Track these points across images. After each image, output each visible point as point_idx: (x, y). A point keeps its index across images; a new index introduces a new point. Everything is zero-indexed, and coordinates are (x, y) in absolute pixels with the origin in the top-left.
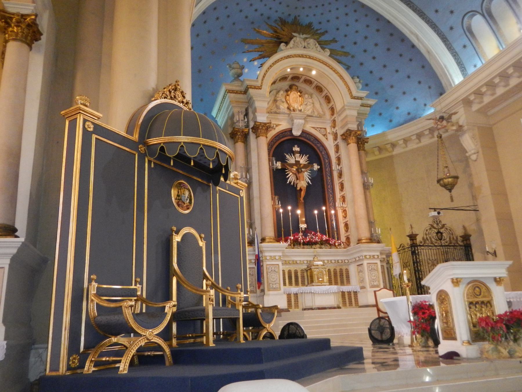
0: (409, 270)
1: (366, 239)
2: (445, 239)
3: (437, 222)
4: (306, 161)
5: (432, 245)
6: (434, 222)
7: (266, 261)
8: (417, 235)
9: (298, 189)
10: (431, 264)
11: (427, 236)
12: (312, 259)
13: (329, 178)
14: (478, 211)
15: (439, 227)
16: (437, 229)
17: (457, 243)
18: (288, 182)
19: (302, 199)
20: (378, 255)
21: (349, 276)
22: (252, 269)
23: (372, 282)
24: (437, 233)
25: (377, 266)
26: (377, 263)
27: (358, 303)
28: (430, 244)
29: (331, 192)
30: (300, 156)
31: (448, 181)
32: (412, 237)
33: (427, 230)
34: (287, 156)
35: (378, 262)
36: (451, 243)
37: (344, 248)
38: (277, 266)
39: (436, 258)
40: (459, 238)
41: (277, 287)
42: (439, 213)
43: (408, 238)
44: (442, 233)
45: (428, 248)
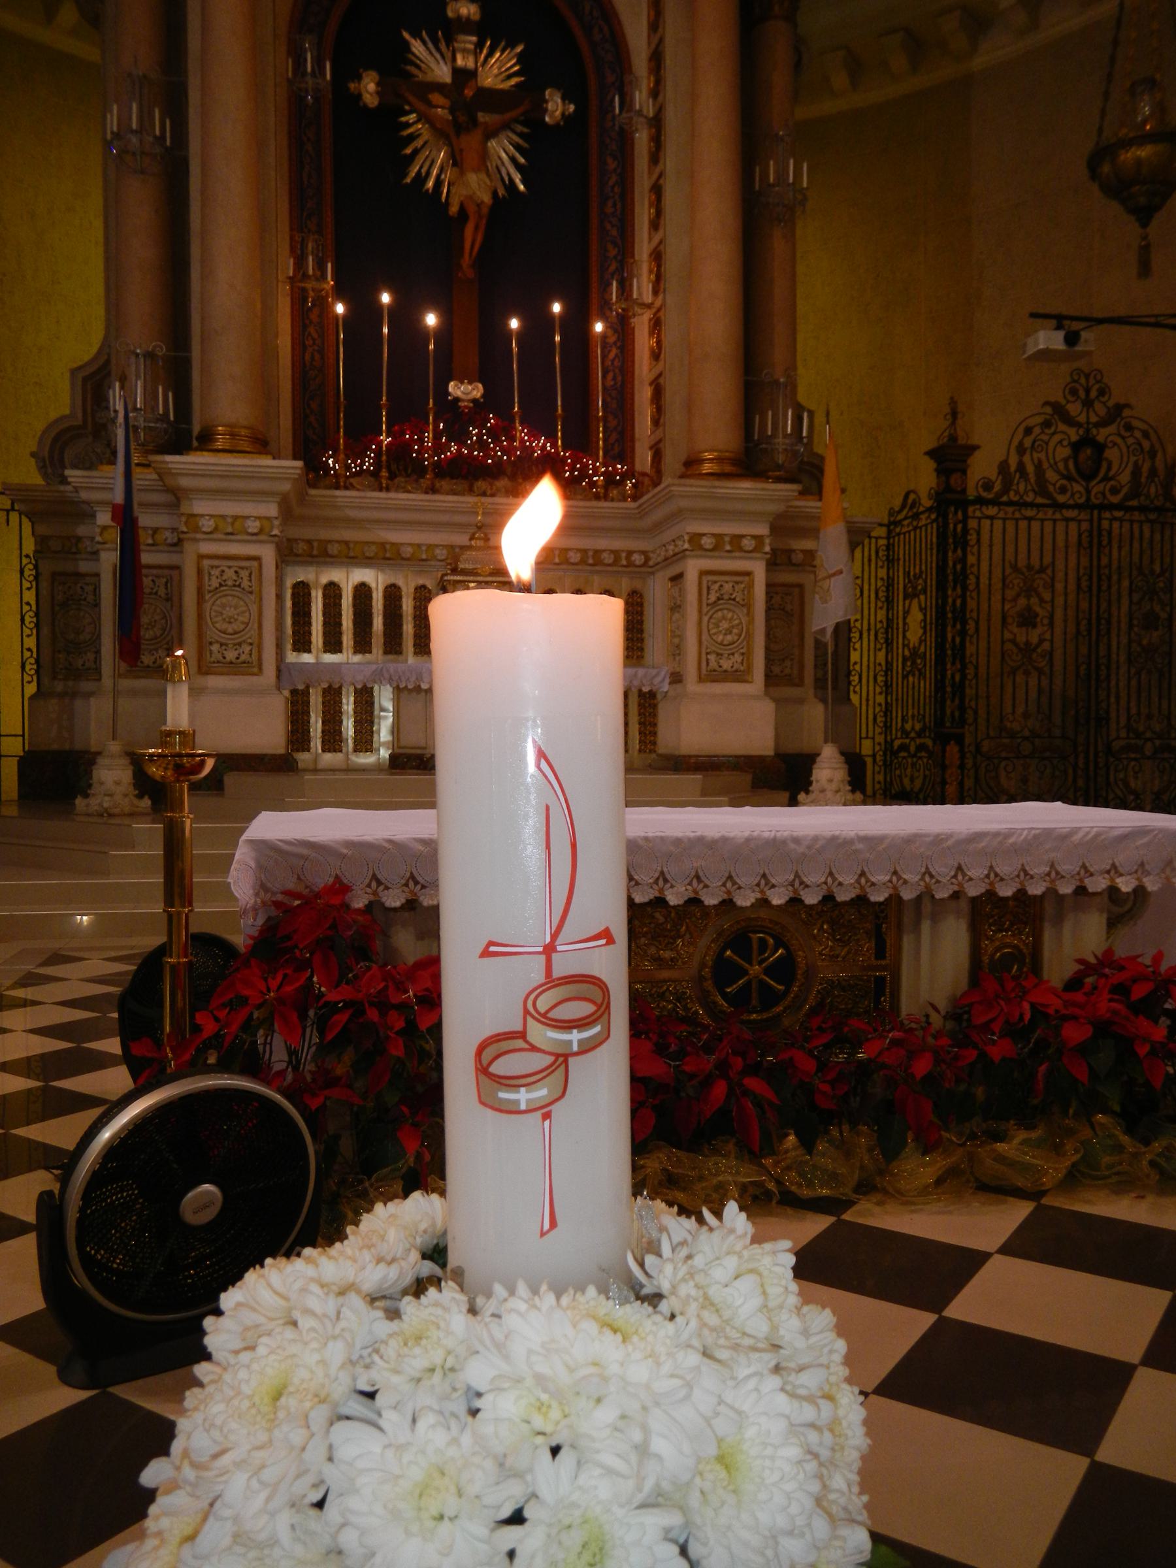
0: (921, 609)
1: (719, 460)
4: (509, 77)
5: (1040, 500)
6: (1074, 392)
7: (196, 540)
9: (454, 209)
11: (1027, 459)
12: (461, 539)
13: (612, 164)
15: (1094, 419)
16: (1078, 425)
18: (408, 180)
19: (466, 261)
20: (758, 539)
21: (641, 622)
22: (166, 572)
23: (712, 657)
24: (1076, 447)
25: (750, 586)
26: (748, 574)
27: (654, 743)
28: (1030, 498)
29: (614, 232)
30: (480, 45)
31: (1139, 162)
34: (417, 47)
35: (759, 570)
36: (1135, 492)
37: (635, 498)
38: (255, 564)
39: (1047, 559)
41: (243, 658)
42: (1072, 339)
43: (930, 465)
44: (1100, 448)
45: (1017, 515)
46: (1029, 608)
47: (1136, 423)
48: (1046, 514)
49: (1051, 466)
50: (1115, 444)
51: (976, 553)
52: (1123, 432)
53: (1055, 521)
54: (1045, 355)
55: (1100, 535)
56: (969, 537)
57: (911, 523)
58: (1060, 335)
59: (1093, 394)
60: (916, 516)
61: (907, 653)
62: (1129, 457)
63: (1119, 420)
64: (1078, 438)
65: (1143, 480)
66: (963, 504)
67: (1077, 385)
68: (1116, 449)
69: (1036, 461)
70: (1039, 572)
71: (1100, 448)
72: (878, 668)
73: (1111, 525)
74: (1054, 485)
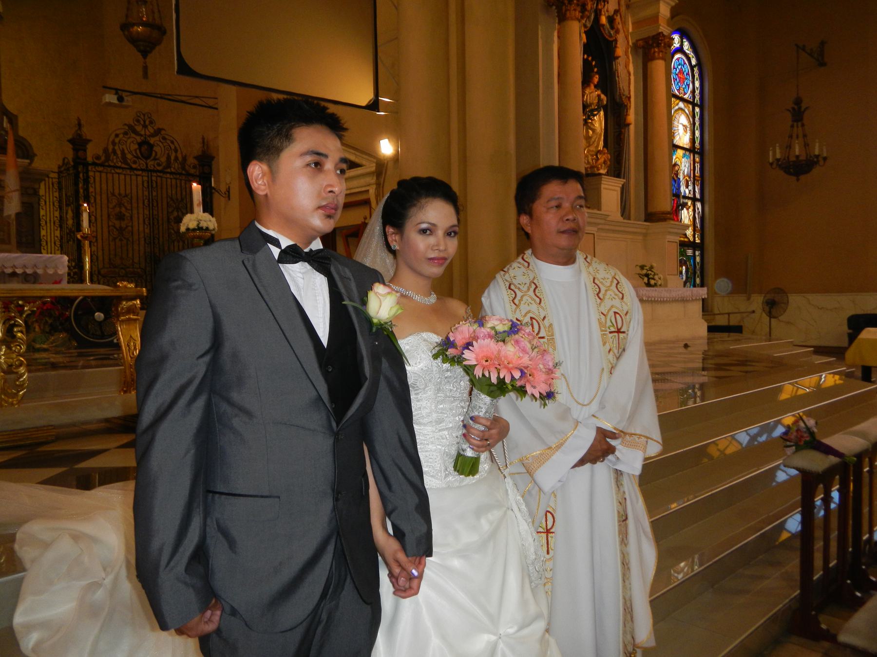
2: (157, 157)
5: (123, 166)
6: (138, 121)
8: (90, 141)
11: (116, 148)
14: (217, 109)
15: (148, 133)
16: (142, 135)
17: (183, 168)
24: (140, 145)
28: (120, 164)
31: (137, 32)
32: (79, 143)
36: (169, 165)
39: (128, 192)
40: (191, 161)
42: (121, 99)
44: (151, 147)
46: (121, 212)
47: (167, 137)
52: (161, 140)
54: (110, 104)
55: (152, 182)
58: (116, 97)
59: (147, 123)
60: (68, 169)
61: (68, 231)
62: (165, 151)
63: (160, 135)
64: (141, 140)
65: (172, 161)
66: (86, 165)
69: (121, 148)
70: (124, 197)
71: (151, 147)
73: (157, 179)
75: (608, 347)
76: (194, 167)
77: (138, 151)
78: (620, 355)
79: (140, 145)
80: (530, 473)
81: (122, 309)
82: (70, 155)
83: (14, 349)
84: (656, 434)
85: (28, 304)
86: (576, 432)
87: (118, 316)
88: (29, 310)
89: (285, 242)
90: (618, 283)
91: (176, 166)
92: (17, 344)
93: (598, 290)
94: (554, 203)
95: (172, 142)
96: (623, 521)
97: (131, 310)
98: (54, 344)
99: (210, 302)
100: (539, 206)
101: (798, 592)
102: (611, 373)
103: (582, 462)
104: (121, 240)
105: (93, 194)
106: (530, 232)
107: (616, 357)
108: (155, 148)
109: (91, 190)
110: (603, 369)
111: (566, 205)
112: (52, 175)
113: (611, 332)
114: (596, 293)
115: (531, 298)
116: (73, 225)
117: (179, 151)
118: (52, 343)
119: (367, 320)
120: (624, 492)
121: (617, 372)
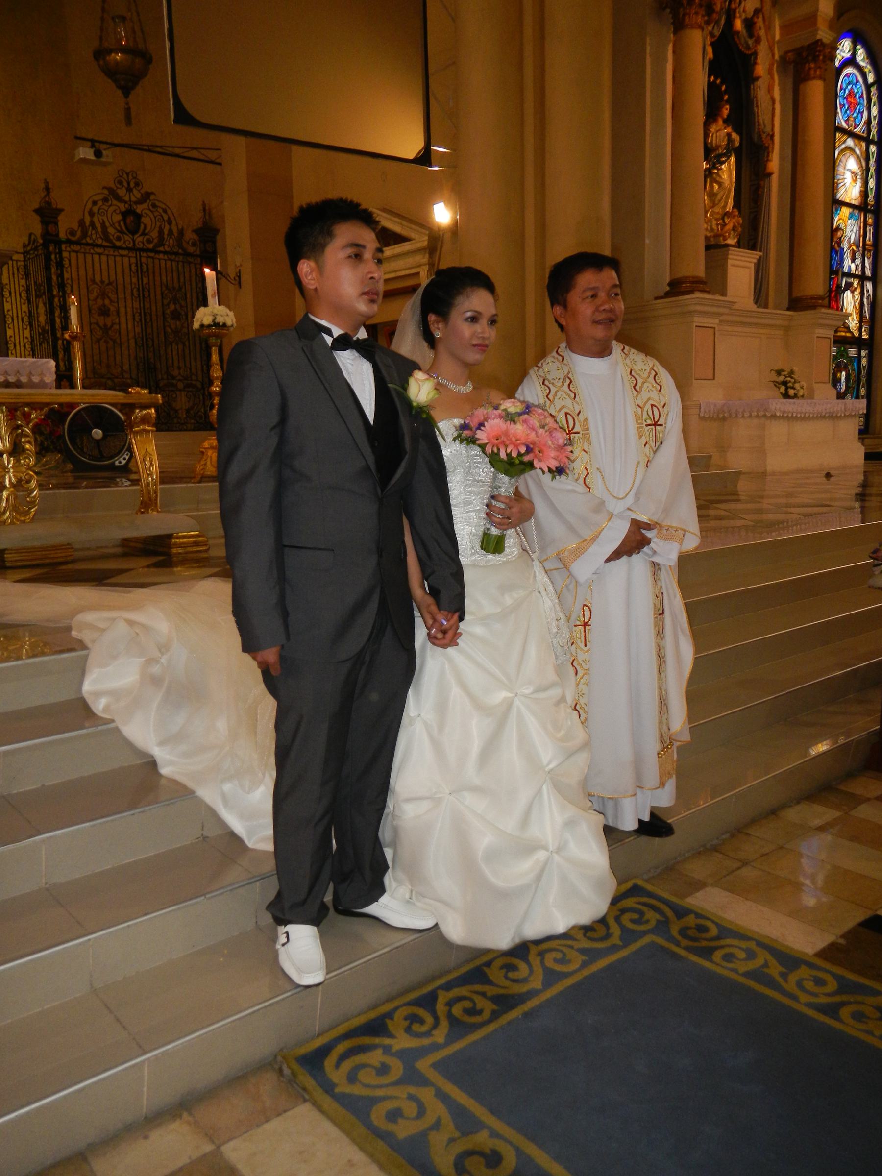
3: (129, 184)
6: (120, 183)
8: (61, 210)
10: (95, 294)
11: (95, 219)
14: (220, 164)
15: (133, 199)
16: (125, 202)
17: (180, 245)
24: (125, 214)
28: (100, 242)
31: (116, 61)
33: (95, 203)
36: (161, 242)
39: (113, 278)
40: (190, 236)
42: (98, 154)
43: (37, 218)
44: (138, 217)
46: (104, 305)
47: (157, 203)
48: (109, 251)
49: (111, 225)
50: (147, 214)
51: (69, 272)
52: (151, 207)
53: (115, 256)
54: (84, 161)
56: (64, 262)
57: (34, 253)
58: (92, 151)
59: (132, 185)
61: (40, 331)
63: (148, 201)
65: (165, 236)
66: (59, 243)
67: (122, 179)
68: (148, 219)
69: (101, 221)
70: (108, 284)
71: (138, 217)
72: (26, 340)
74: (113, 236)
75: (644, 440)
76: (194, 244)
77: (122, 223)
78: (657, 449)
79: (125, 214)
80: (566, 567)
81: (136, 418)
82: (37, 229)
83: (22, 461)
84: (693, 525)
85: (34, 412)
86: (609, 524)
87: (131, 428)
88: (36, 418)
89: (337, 332)
90: (656, 374)
91: (170, 243)
92: (26, 455)
93: (634, 382)
94: (590, 293)
95: (165, 211)
96: (659, 615)
97: (144, 420)
98: (47, 467)
99: (278, 382)
100: (575, 297)
101: (879, 727)
102: (647, 467)
103: (616, 555)
104: (106, 342)
105: (69, 281)
106: (564, 324)
107: (653, 451)
108: (143, 219)
109: (66, 276)
110: (638, 463)
111: (602, 295)
112: (15, 257)
113: (647, 425)
114: (632, 385)
115: (565, 393)
116: (46, 323)
117: (174, 222)
118: (45, 466)
119: (407, 402)
120: (661, 587)
121: (652, 466)
